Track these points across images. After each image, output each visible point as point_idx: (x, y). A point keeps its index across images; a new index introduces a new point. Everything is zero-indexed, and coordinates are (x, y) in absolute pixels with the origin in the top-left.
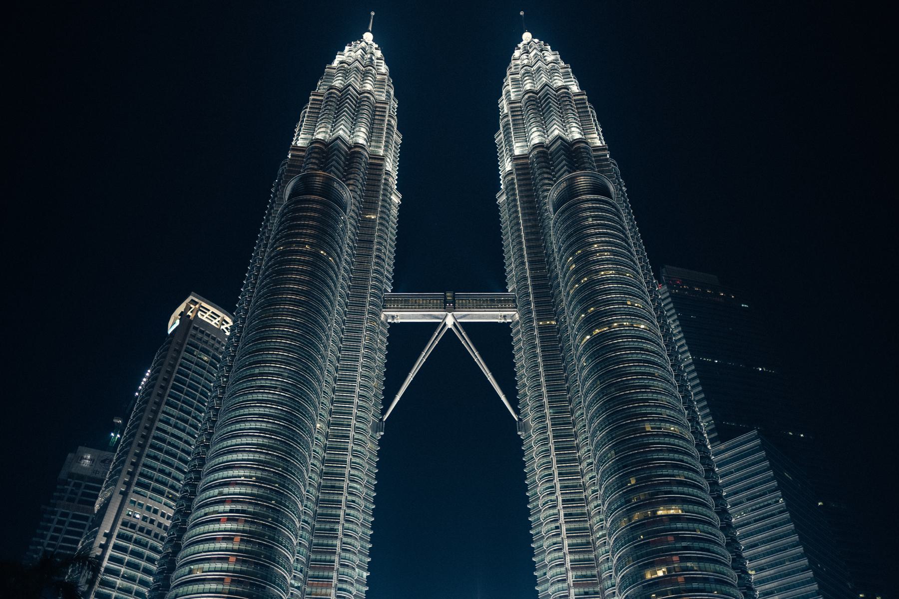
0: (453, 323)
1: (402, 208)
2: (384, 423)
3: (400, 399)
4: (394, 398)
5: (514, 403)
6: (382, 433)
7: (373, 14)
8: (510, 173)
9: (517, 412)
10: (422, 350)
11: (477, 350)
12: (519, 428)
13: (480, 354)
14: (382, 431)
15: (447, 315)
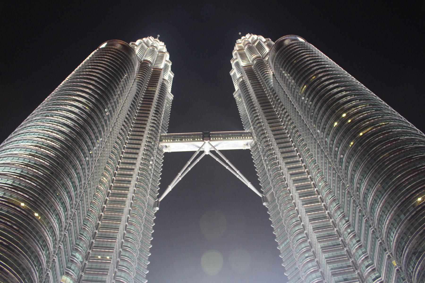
0: (209, 150)
1: (173, 101)
2: (159, 203)
3: (172, 190)
4: (166, 188)
5: (258, 188)
6: (158, 209)
7: (159, 36)
8: (242, 77)
9: (261, 192)
10: (188, 160)
11: (227, 158)
12: (264, 200)
13: (230, 161)
14: (158, 207)
15: (205, 143)
